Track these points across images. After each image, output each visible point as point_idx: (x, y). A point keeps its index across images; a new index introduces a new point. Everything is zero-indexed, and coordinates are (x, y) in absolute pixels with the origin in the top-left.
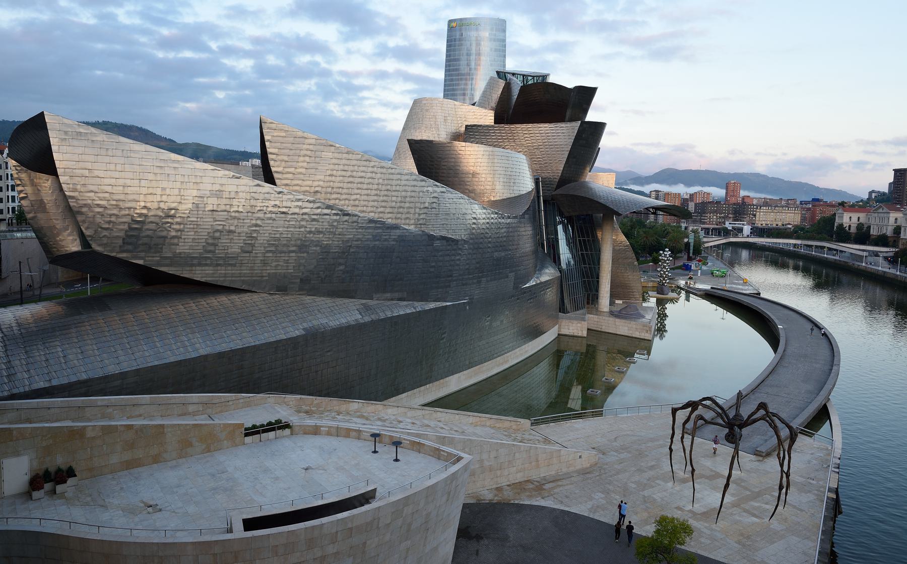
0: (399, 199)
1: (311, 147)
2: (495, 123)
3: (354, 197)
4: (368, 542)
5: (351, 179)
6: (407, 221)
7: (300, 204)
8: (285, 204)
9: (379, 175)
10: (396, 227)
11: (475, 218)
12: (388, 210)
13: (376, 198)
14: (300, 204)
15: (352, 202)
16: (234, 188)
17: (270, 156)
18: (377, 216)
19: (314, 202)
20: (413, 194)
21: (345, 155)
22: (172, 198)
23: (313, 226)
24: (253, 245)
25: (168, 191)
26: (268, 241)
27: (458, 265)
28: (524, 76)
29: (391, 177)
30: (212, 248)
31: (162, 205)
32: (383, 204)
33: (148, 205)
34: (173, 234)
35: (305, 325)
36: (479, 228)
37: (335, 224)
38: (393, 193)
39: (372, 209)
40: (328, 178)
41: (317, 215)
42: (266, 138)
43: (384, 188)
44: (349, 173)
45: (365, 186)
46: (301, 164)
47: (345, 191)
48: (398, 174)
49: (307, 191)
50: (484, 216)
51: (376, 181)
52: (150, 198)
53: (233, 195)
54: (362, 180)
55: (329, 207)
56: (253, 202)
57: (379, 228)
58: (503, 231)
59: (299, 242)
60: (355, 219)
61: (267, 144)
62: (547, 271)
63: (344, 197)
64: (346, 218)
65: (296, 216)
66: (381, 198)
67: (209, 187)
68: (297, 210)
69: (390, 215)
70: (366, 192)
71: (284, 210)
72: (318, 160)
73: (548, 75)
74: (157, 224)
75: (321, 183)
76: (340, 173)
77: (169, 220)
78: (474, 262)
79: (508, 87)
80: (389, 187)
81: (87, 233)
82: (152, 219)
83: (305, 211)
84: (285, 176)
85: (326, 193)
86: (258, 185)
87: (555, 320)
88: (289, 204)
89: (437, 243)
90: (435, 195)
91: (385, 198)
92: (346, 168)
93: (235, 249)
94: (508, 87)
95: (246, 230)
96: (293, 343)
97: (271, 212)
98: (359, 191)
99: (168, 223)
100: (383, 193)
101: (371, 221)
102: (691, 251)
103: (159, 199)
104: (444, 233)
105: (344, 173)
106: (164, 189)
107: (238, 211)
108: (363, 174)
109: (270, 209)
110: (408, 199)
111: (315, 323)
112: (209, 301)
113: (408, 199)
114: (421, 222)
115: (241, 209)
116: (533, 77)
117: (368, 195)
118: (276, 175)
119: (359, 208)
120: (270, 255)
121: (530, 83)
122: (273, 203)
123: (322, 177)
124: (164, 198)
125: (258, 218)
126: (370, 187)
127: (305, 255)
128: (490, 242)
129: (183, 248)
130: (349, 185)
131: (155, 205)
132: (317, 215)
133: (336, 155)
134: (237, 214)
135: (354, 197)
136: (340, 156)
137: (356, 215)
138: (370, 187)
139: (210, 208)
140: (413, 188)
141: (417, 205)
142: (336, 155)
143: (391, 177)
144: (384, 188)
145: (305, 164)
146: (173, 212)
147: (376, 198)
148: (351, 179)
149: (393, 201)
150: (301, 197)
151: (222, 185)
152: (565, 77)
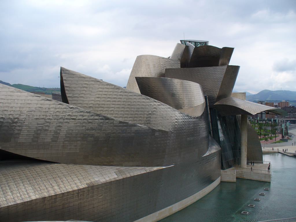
0: (136, 110)
1: (87, 82)
2: (181, 67)
3: (111, 109)
5: (109, 99)
6: (140, 122)
7: (82, 114)
8: (74, 114)
9: (124, 97)
10: (134, 125)
11: (176, 119)
12: (130, 116)
13: (123, 109)
14: (82, 114)
15: (110, 112)
16: (47, 106)
17: (66, 88)
18: (123, 119)
19: (89, 112)
20: (143, 107)
21: (106, 86)
22: (16, 113)
23: (90, 126)
24: (57, 137)
25: (14, 109)
26: (65, 135)
28: (195, 42)
29: (131, 97)
31: (11, 116)
32: (127, 113)
33: (4, 116)
34: (16, 132)
35: (88, 182)
36: (179, 124)
37: (101, 124)
38: (132, 107)
39: (121, 116)
40: (97, 99)
41: (91, 120)
42: (64, 78)
43: (127, 103)
44: (109, 96)
45: (117, 103)
46: (82, 92)
47: (106, 106)
48: (135, 96)
49: (85, 107)
50: (181, 118)
51: (123, 100)
52: (6, 112)
53: (47, 110)
54: (115, 100)
55: (98, 115)
56: (58, 114)
57: (125, 126)
58: (191, 126)
59: (82, 135)
60: (112, 121)
61: (64, 81)
62: (214, 147)
63: (105, 109)
64: (107, 121)
65: (80, 121)
66: (126, 109)
67: (35, 106)
68: (81, 117)
69: (131, 119)
70: (117, 106)
71: (74, 117)
72: (91, 89)
73: (208, 42)
74: (8, 127)
75: (93, 102)
76: (103, 96)
77: (15, 125)
79: (187, 48)
80: (130, 103)
82: (6, 124)
83: (85, 117)
84: (74, 99)
85: (96, 107)
86: (60, 104)
87: (220, 175)
88: (76, 114)
89: (157, 134)
90: (155, 107)
91: (128, 109)
92: (106, 93)
93: (48, 140)
94: (187, 48)
95: (54, 129)
96: (80, 192)
97: (67, 119)
98: (113, 106)
99: (14, 126)
100: (126, 106)
101: (121, 122)
102: (284, 133)
103: (9, 113)
104: (160, 128)
105: (105, 96)
106: (12, 107)
107: (49, 119)
108: (115, 96)
109: (66, 117)
110: (140, 110)
111: (93, 180)
112: (35, 169)
114: (147, 122)
115: (51, 118)
116: (200, 43)
117: (118, 108)
118: (68, 99)
119: (114, 115)
120: (67, 142)
121: (198, 46)
122: (68, 114)
123: (93, 99)
124: (12, 113)
125: (60, 122)
126: (119, 103)
127: (86, 142)
128: (185, 132)
129: (22, 139)
130: (109, 103)
131: (8, 116)
132: (91, 120)
133: (100, 86)
134: (49, 121)
135: (111, 109)
136: (103, 86)
137: (112, 119)
138: (119, 103)
139: (36, 117)
141: (145, 112)
142: (100, 86)
143: (131, 97)
144: (127, 103)
145: (84, 92)
146: (16, 120)
147: (123, 109)
148: (109, 99)
149: (132, 111)
150: (82, 110)
151: (41, 104)
152: (217, 42)
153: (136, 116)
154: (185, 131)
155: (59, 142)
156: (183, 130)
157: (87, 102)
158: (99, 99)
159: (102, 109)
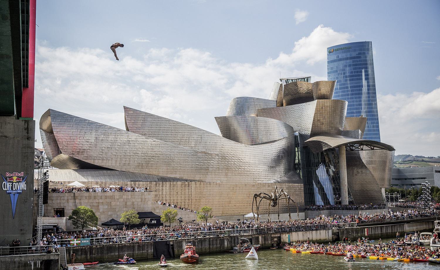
1: (143, 117)
4: (112, 203)
27: (212, 165)
30: (102, 153)
34: (88, 148)
44: (159, 126)
63: (157, 135)
64: (154, 143)
75: (147, 131)
78: (222, 165)
80: (177, 131)
81: (60, 148)
113: (185, 136)
116: (292, 80)
133: (154, 119)
139: (101, 139)
140: (188, 131)
142: (154, 119)
153: (182, 141)
154: (233, 156)
155: (118, 156)
156: (230, 154)
157: (143, 131)
158: (152, 129)
159: (155, 135)
